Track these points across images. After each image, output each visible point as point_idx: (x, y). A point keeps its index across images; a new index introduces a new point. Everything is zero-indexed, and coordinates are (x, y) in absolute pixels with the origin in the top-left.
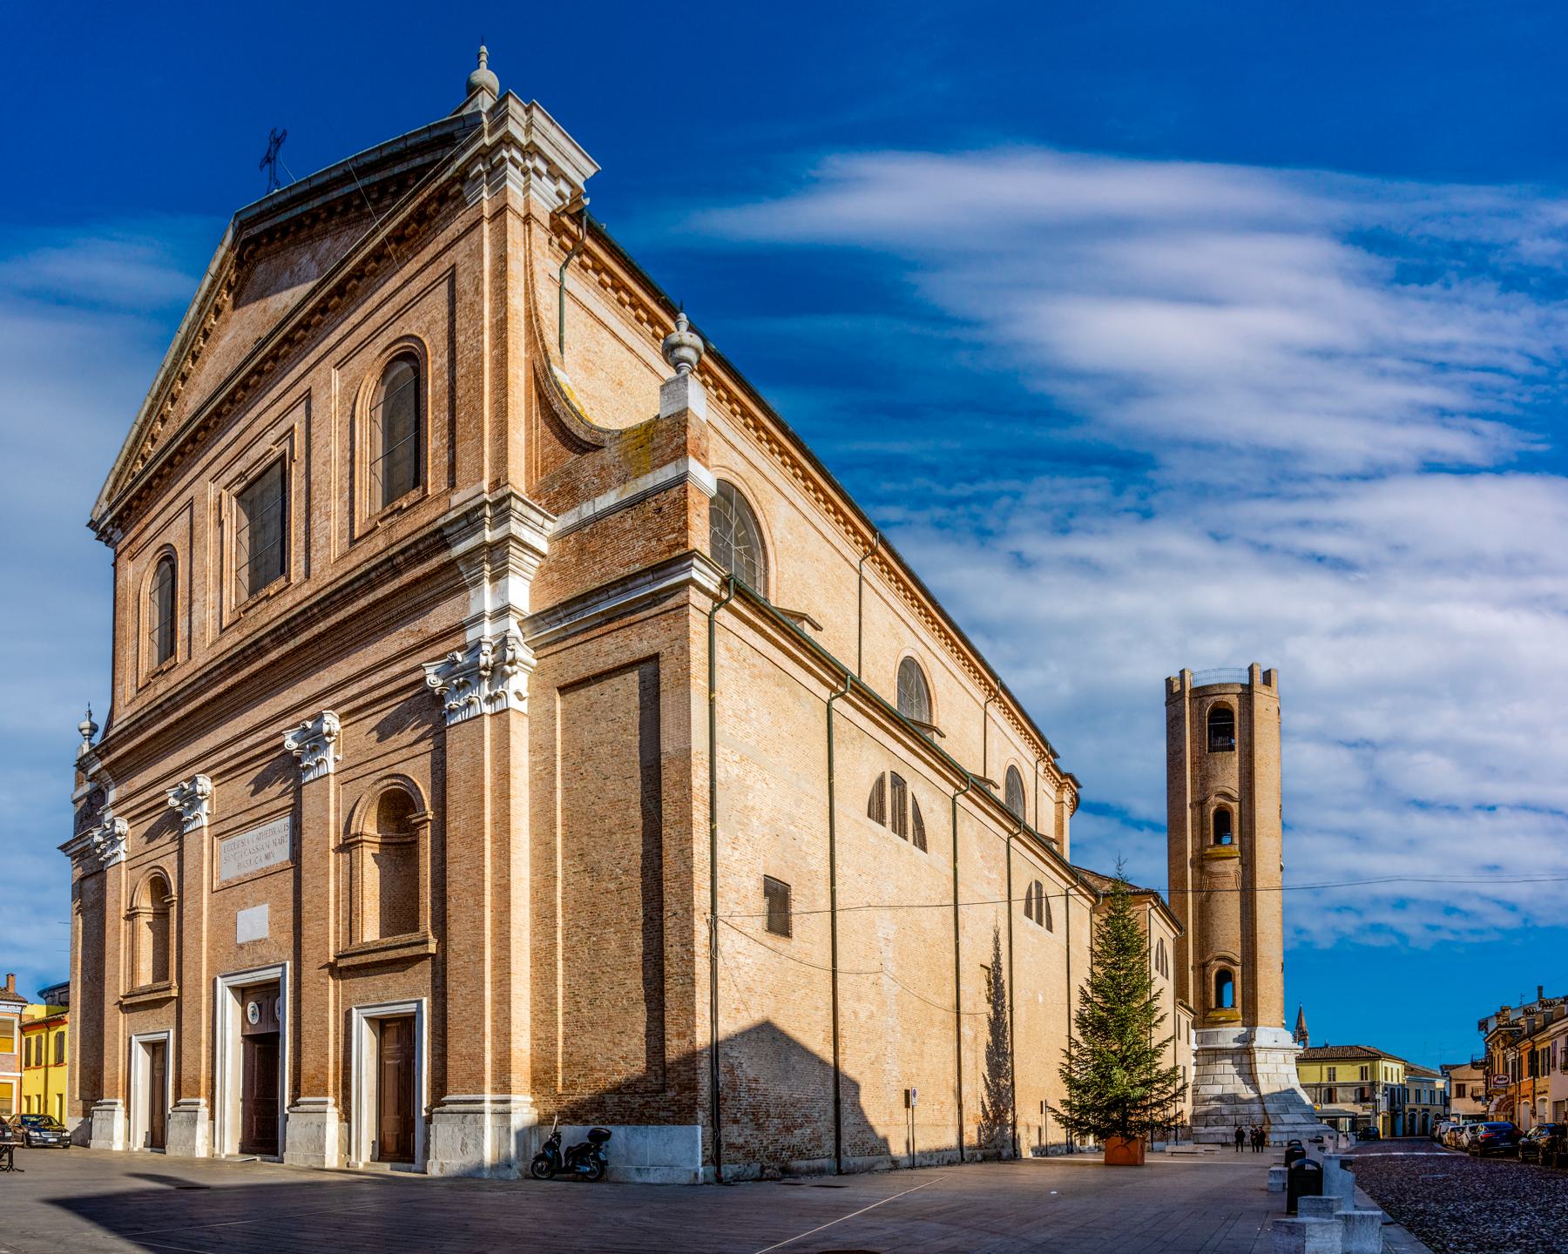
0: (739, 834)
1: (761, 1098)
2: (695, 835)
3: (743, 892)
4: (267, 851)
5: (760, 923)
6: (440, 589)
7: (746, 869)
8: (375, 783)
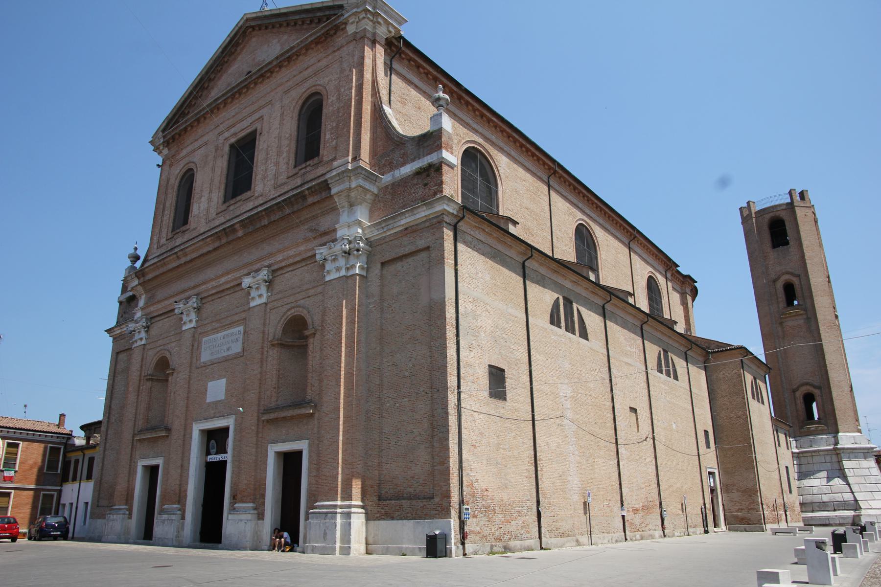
0: (473, 342)
2: (448, 345)
3: (476, 375)
4: (228, 346)
5: (486, 393)
6: (325, 209)
7: (478, 362)
8: (288, 311)
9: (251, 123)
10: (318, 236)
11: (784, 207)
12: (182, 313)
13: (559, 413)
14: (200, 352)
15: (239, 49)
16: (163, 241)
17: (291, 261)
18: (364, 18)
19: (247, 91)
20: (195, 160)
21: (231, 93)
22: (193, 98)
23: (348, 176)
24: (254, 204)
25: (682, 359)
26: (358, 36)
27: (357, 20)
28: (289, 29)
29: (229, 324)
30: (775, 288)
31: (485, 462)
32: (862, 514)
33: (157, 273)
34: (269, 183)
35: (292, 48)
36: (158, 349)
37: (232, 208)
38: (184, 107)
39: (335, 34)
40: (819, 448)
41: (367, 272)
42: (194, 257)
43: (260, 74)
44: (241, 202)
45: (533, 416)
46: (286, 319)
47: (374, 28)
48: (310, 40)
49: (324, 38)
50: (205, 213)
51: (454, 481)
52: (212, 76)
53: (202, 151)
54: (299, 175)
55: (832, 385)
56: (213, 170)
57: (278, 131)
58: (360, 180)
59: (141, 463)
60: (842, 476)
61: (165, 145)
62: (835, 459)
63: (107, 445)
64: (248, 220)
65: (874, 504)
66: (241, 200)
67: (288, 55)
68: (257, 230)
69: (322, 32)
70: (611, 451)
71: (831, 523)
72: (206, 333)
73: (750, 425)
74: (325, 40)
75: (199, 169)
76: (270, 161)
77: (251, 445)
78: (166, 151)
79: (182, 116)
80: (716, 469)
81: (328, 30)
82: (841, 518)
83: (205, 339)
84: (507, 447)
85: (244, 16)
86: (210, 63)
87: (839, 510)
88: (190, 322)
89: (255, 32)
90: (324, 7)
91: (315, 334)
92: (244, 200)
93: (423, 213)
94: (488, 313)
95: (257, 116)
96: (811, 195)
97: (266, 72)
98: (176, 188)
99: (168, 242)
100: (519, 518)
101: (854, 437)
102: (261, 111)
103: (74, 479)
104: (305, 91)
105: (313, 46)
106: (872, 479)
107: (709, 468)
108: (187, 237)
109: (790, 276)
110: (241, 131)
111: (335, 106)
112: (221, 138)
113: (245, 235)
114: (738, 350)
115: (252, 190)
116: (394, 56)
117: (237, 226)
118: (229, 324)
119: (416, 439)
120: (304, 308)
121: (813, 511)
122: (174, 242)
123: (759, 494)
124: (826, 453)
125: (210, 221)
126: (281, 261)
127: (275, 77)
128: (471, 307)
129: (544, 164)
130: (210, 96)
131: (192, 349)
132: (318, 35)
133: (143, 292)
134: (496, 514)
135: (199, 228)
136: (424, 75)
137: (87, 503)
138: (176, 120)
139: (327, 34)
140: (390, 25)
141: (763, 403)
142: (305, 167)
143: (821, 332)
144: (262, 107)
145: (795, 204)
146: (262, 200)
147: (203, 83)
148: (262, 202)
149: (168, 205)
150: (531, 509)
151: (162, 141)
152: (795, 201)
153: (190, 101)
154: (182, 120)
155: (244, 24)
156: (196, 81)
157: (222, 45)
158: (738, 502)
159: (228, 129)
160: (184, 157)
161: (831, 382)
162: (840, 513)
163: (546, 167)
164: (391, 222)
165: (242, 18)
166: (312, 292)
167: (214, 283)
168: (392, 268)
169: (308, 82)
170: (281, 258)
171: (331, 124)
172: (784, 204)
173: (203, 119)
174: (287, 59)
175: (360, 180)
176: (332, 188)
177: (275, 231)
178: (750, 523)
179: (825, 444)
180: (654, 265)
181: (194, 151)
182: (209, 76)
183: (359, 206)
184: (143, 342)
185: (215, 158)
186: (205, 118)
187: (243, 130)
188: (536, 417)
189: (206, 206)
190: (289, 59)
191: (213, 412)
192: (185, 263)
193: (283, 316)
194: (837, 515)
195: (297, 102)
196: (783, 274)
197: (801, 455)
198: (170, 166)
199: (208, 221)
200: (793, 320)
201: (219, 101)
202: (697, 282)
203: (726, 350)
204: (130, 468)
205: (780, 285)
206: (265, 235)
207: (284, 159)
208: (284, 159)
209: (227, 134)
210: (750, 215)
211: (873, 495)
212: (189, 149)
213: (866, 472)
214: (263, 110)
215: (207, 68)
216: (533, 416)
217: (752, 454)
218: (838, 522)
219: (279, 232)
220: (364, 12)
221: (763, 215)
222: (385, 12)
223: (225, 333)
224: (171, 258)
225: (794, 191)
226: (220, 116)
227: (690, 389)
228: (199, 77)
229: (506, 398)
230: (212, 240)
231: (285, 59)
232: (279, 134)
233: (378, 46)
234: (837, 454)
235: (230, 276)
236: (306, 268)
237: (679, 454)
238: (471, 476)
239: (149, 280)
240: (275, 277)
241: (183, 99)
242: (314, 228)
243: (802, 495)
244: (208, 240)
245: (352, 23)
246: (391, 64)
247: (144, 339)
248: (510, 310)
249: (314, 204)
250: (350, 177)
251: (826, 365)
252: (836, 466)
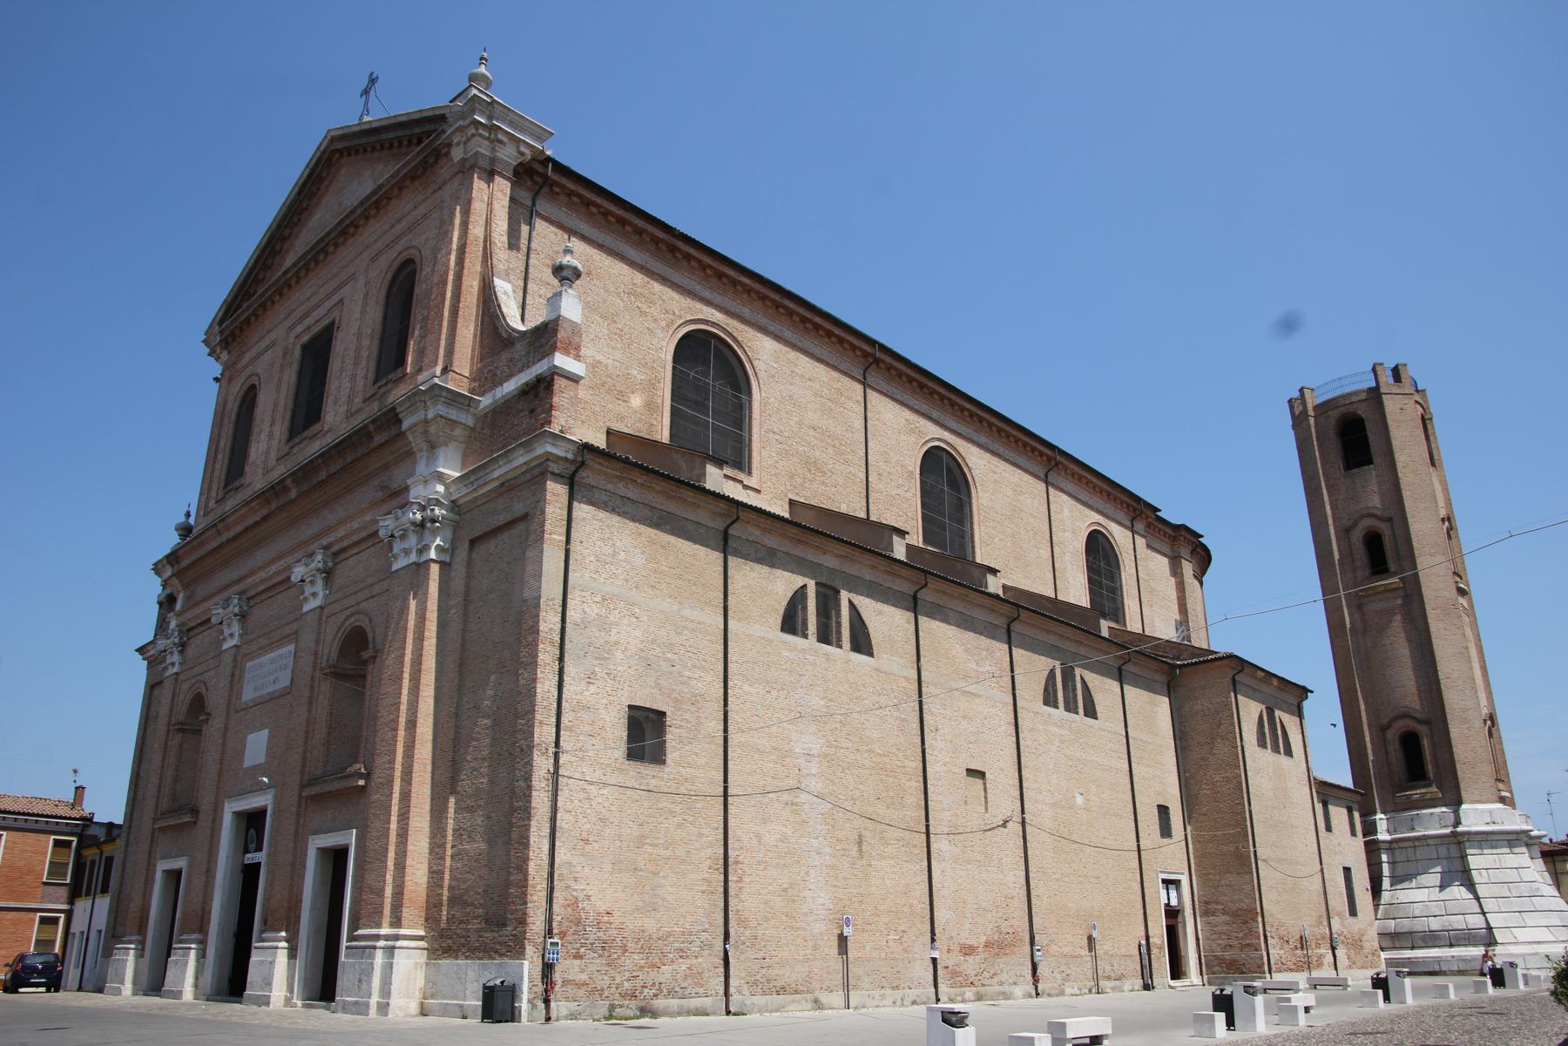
0: (597, 669)
1: (615, 932)
7: (605, 701)
8: (346, 619)
11: (1364, 396)
12: (221, 623)
13: (792, 783)
14: (242, 685)
15: (323, 187)
16: (212, 503)
17: (355, 538)
18: (474, 135)
19: (326, 257)
22: (261, 268)
25: (1111, 678)
26: (468, 165)
29: (279, 641)
30: (1349, 542)
31: (608, 867)
32: (1496, 952)
34: (341, 408)
36: (193, 681)
39: (436, 162)
40: (1426, 833)
41: (452, 554)
43: (339, 230)
44: (305, 443)
45: (726, 788)
46: (344, 632)
47: (493, 150)
49: (421, 170)
51: (535, 898)
53: (267, 356)
54: (378, 396)
55: (1449, 717)
56: (279, 387)
57: (358, 324)
58: (439, 407)
59: (162, 866)
60: (1468, 883)
62: (1454, 852)
63: (132, 836)
65: (1522, 934)
67: (374, 199)
70: (915, 846)
71: (1444, 969)
72: (251, 656)
73: (1245, 796)
75: (262, 385)
77: (289, 837)
78: (225, 356)
80: (1183, 874)
81: (425, 157)
82: (1462, 960)
83: (249, 665)
84: (661, 841)
87: (1459, 945)
88: (232, 636)
91: (376, 657)
93: (521, 459)
94: (635, 620)
95: (336, 298)
96: (1411, 371)
97: (348, 226)
98: (234, 416)
100: (680, 960)
101: (1490, 812)
103: (88, 894)
104: (396, 258)
105: (408, 182)
106: (1522, 888)
107: (1161, 872)
109: (1374, 519)
110: (316, 323)
112: (293, 335)
113: (300, 496)
114: (1225, 662)
115: (322, 421)
116: (539, 190)
118: (279, 641)
119: (494, 828)
120: (365, 614)
121: (1413, 948)
123: (1260, 919)
124: (1439, 841)
126: (341, 539)
128: (597, 611)
129: (854, 348)
131: (232, 680)
132: (413, 165)
134: (627, 954)
135: (254, 484)
136: (601, 216)
137: (100, 931)
138: (238, 305)
140: (521, 143)
141: (1289, 752)
142: (386, 384)
143: (1429, 621)
145: (1382, 390)
146: (331, 437)
149: (222, 444)
150: (711, 946)
151: (218, 339)
152: (1381, 385)
155: (328, 147)
157: (297, 182)
158: (1224, 933)
160: (246, 366)
161: (1447, 711)
162: (1461, 951)
163: (858, 353)
164: (481, 474)
165: (325, 137)
166: (377, 589)
167: (262, 574)
168: (482, 550)
172: (1364, 391)
173: (269, 304)
174: (376, 204)
175: (439, 407)
176: (403, 419)
178: (1244, 970)
179: (1438, 826)
180: (1105, 511)
181: (259, 355)
183: (443, 448)
184: (175, 670)
185: (282, 367)
188: (730, 792)
189: (265, 446)
190: (377, 205)
191: (249, 783)
192: (228, 541)
193: (340, 628)
194: (1454, 954)
196: (1362, 517)
197: (1395, 845)
199: (267, 471)
200: (1380, 600)
202: (1202, 536)
203: (1204, 662)
204: (147, 875)
205: (1357, 536)
207: (362, 369)
208: (362, 369)
209: (299, 329)
210: (1305, 412)
211: (1523, 919)
213: (1512, 875)
216: (726, 788)
217: (1248, 847)
218: (1456, 968)
220: (472, 126)
221: (1328, 411)
222: (511, 124)
223: (272, 655)
224: (210, 533)
225: (1382, 367)
227: (1127, 732)
229: (665, 760)
231: (371, 205)
232: (359, 328)
233: (498, 179)
234: (1459, 843)
236: (373, 549)
237: (1088, 849)
238: (575, 890)
239: (185, 569)
240: (337, 564)
241: (247, 270)
243: (1394, 919)
246: (534, 205)
247: (177, 663)
248: (687, 612)
249: (382, 445)
250: (425, 402)
251: (1439, 680)
252: (1457, 865)
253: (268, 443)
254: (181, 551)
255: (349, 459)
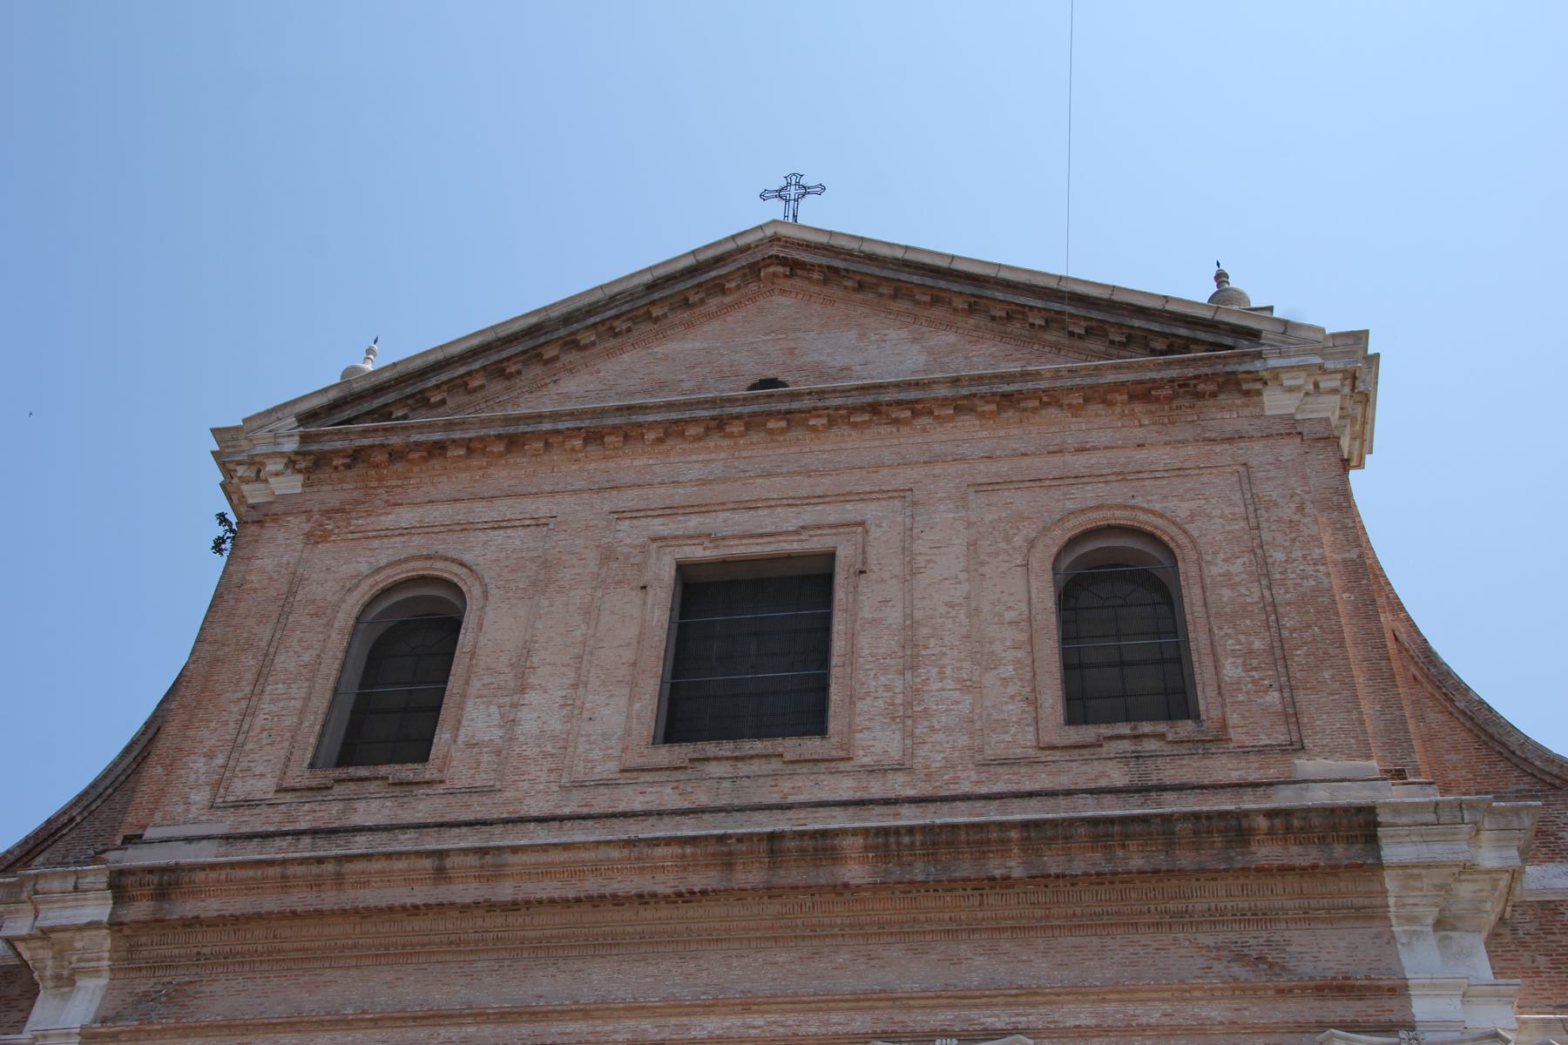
9: (803, 528)
10: (1304, 989)
15: (713, 303)
16: (263, 787)
18: (1335, 391)
20: (467, 557)
21: (715, 412)
22: (484, 368)
23: (1475, 823)
24: (856, 790)
27: (1311, 387)
28: (971, 321)
33: (270, 903)
35: (1025, 376)
37: (715, 769)
38: (433, 382)
39: (1214, 395)
42: (544, 895)
44: (775, 765)
48: (1111, 378)
50: (549, 748)
52: (586, 338)
61: (302, 465)
64: (918, 838)
66: (781, 756)
67: (1006, 388)
68: (952, 885)
69: (1173, 373)
74: (1169, 399)
75: (493, 591)
76: (934, 671)
78: (291, 484)
79: (409, 402)
81: (1197, 377)
85: (768, 224)
86: (593, 299)
89: (797, 282)
90: (1167, 312)
92: (792, 762)
95: (831, 514)
97: (899, 403)
99: (289, 797)
102: (849, 506)
104: (1083, 511)
105: (1118, 397)
108: (423, 808)
111: (1243, 590)
112: (629, 534)
117: (852, 844)
122: (336, 808)
125: (581, 785)
127: (924, 430)
130: (553, 389)
133: (105, 963)
139: (1180, 386)
144: (863, 497)
147: (542, 340)
148: (911, 793)
149: (286, 661)
151: (291, 445)
153: (469, 373)
154: (405, 417)
155: (758, 244)
156: (516, 327)
159: (670, 511)
160: (407, 532)
165: (761, 227)
169: (1089, 488)
170: (1092, 1022)
171: (1242, 637)
173: (541, 445)
177: (1039, 913)
181: (466, 527)
182: (577, 332)
186: (548, 445)
187: (761, 536)
190: (1008, 401)
195: (1046, 530)
198: (308, 535)
201: (650, 418)
206: (980, 915)
207: (1005, 682)
209: (659, 526)
212: (440, 513)
214: (860, 505)
215: (572, 307)
219: (1056, 923)
226: (626, 462)
228: (534, 320)
230: (683, 856)
231: (994, 394)
235: (759, 1021)
239: (191, 923)
241: (440, 356)
242: (1254, 954)
244: (660, 851)
245: (1290, 390)
249: (1285, 870)
250: (1478, 831)
253: (568, 719)
254: (200, 876)
255: (1137, 862)
